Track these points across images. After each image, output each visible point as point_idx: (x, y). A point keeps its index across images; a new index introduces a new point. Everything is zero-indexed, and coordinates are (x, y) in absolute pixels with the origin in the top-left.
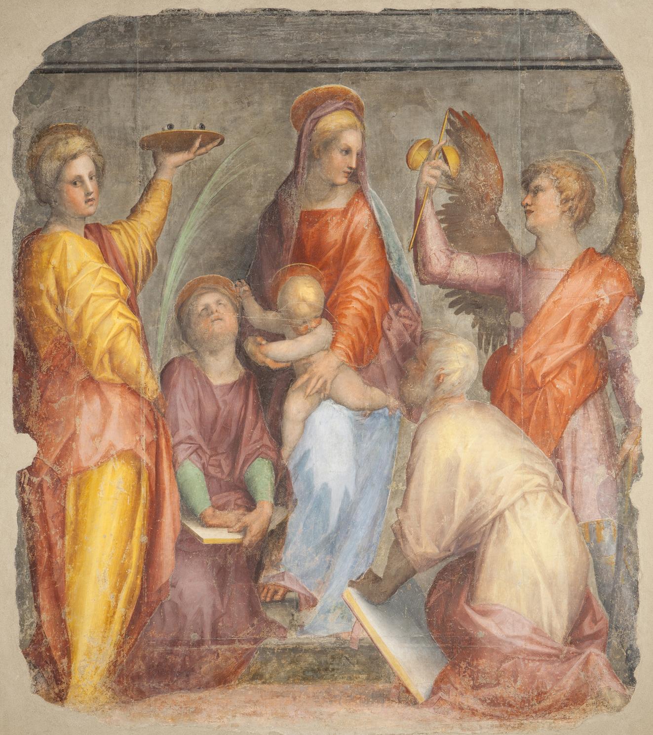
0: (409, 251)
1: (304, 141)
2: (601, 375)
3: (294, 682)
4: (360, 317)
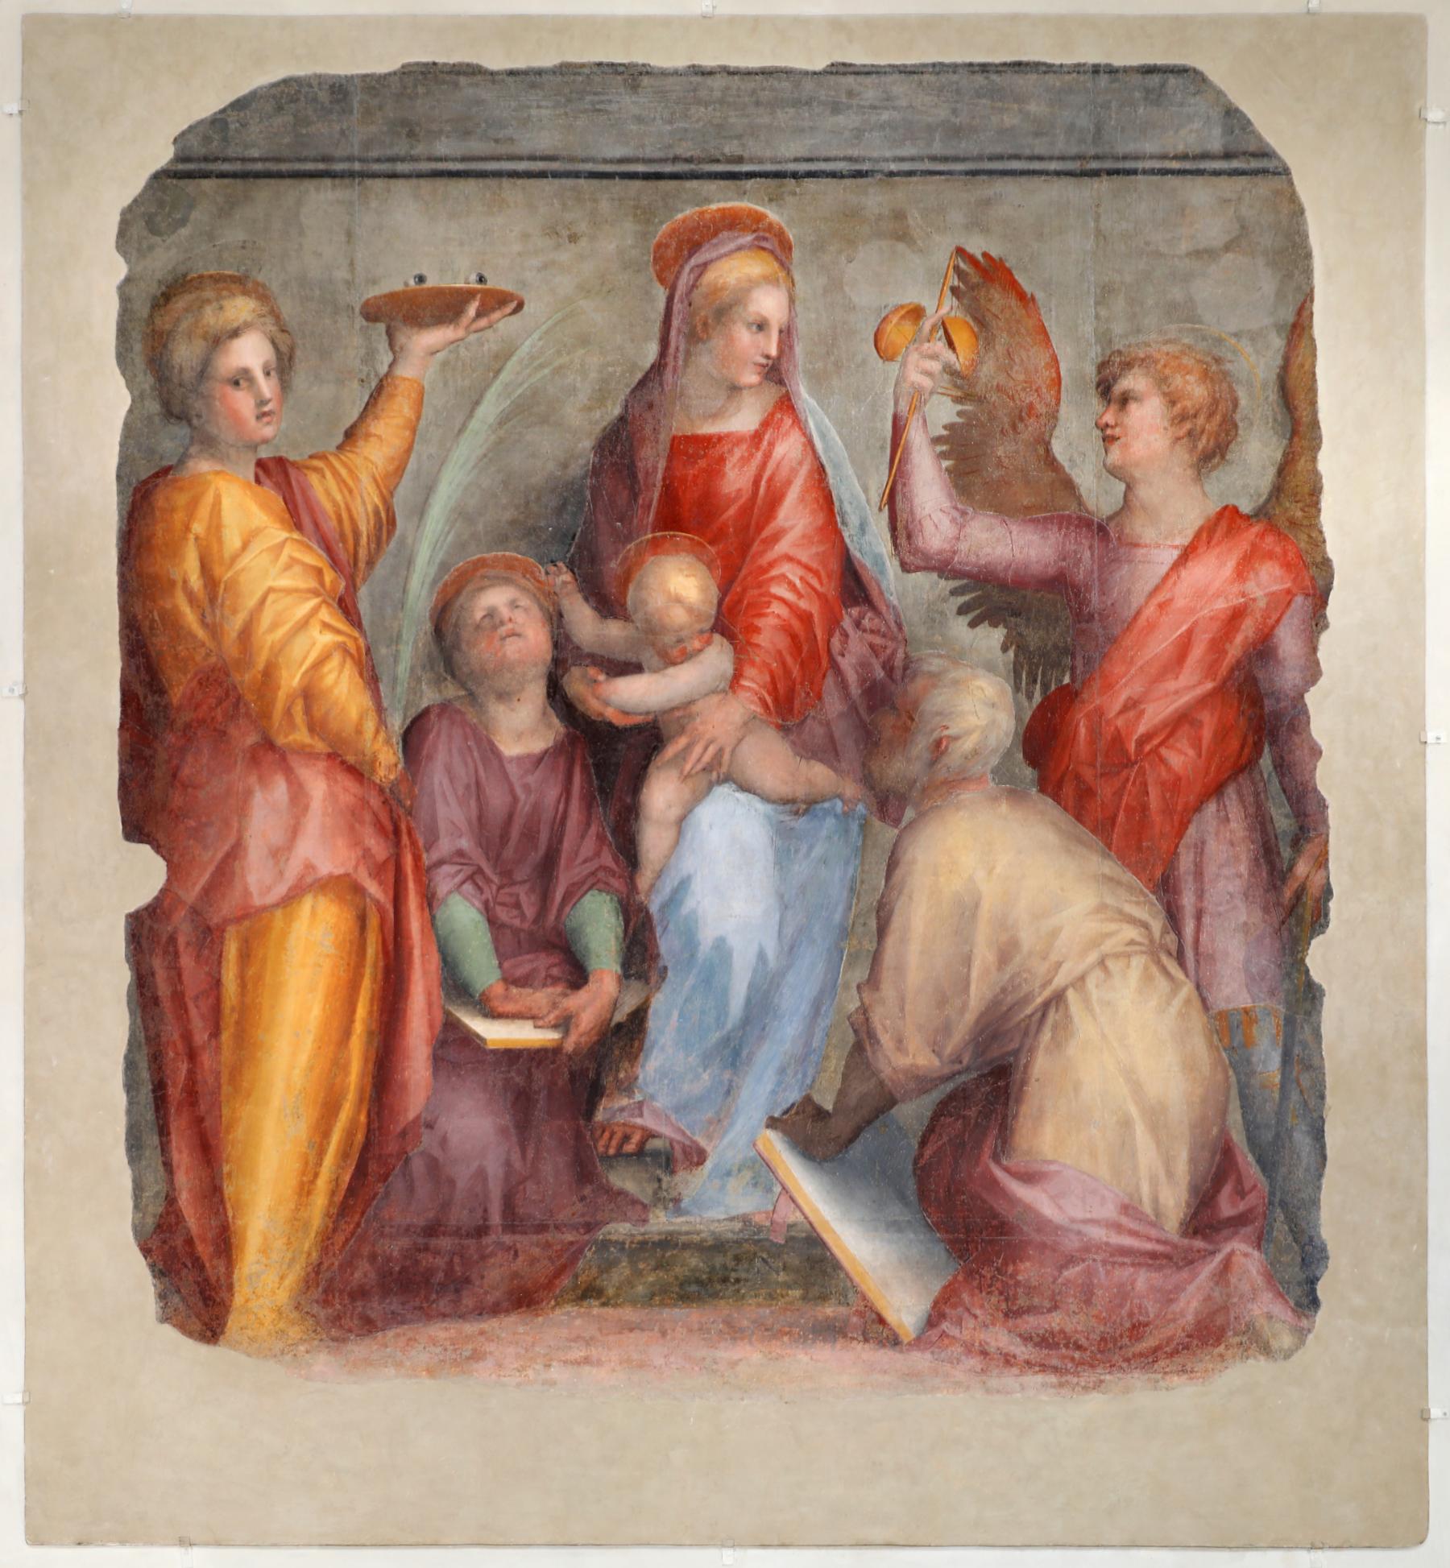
0: (880, 509)
1: (677, 306)
3: (663, 1304)
4: (786, 630)
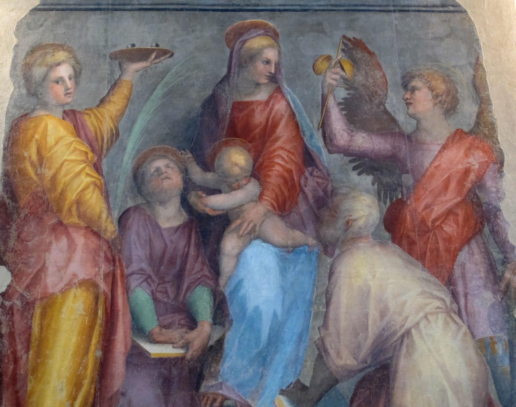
0: (318, 130)
1: (234, 54)
2: (479, 221)
4: (281, 176)
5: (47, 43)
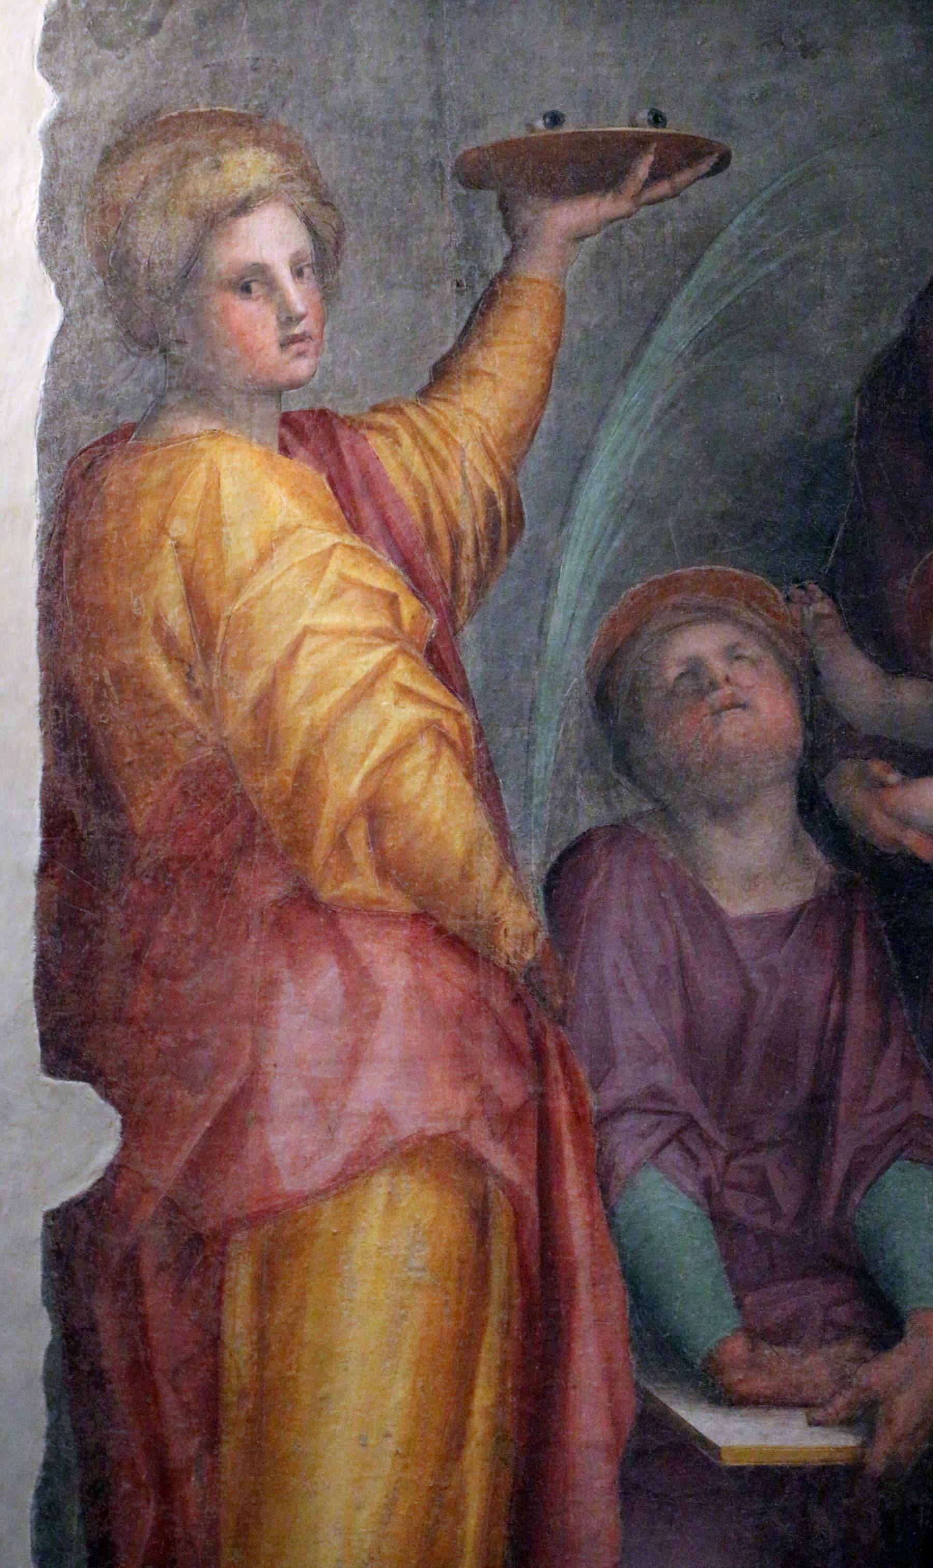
5: (185, 107)
